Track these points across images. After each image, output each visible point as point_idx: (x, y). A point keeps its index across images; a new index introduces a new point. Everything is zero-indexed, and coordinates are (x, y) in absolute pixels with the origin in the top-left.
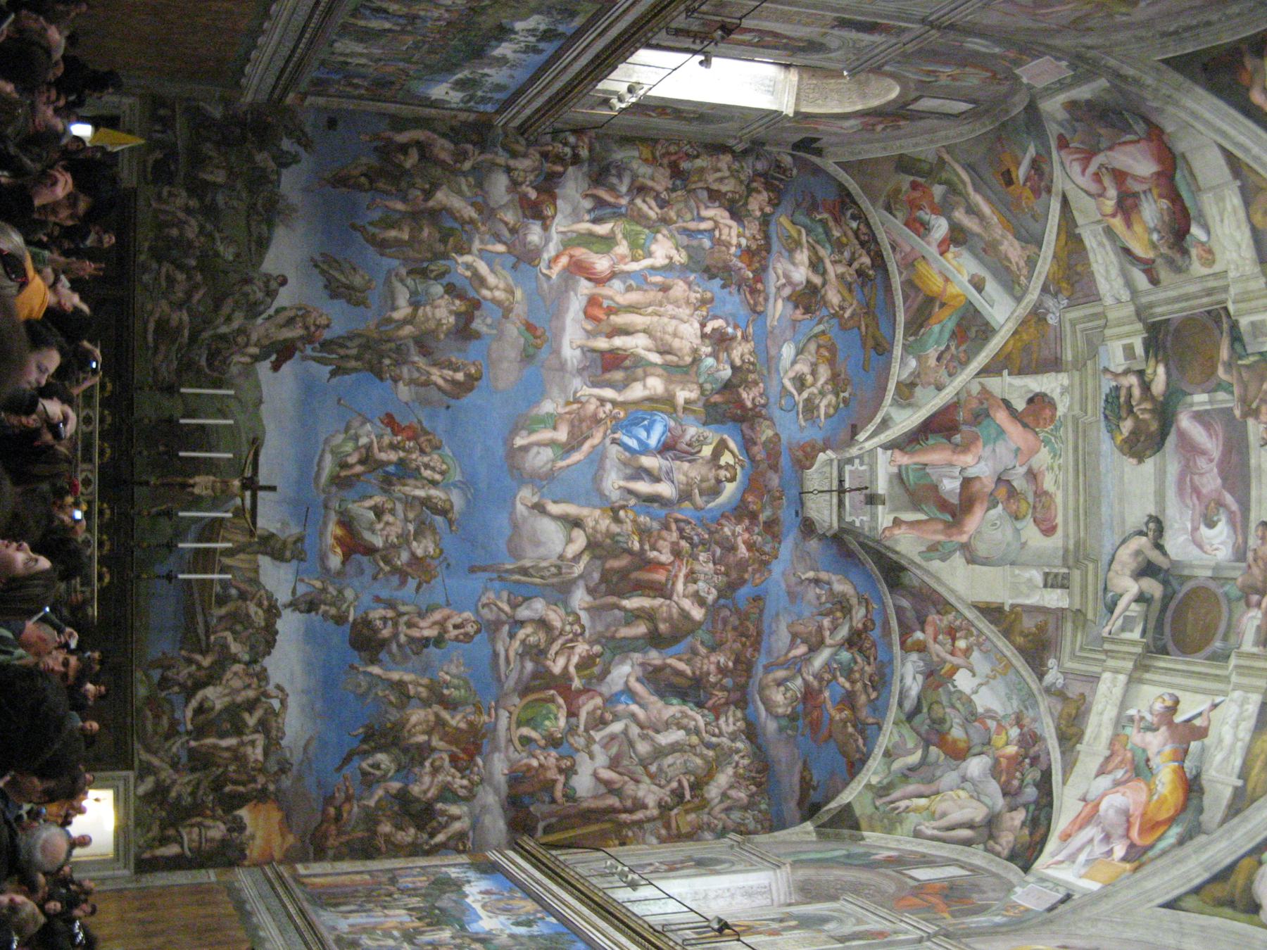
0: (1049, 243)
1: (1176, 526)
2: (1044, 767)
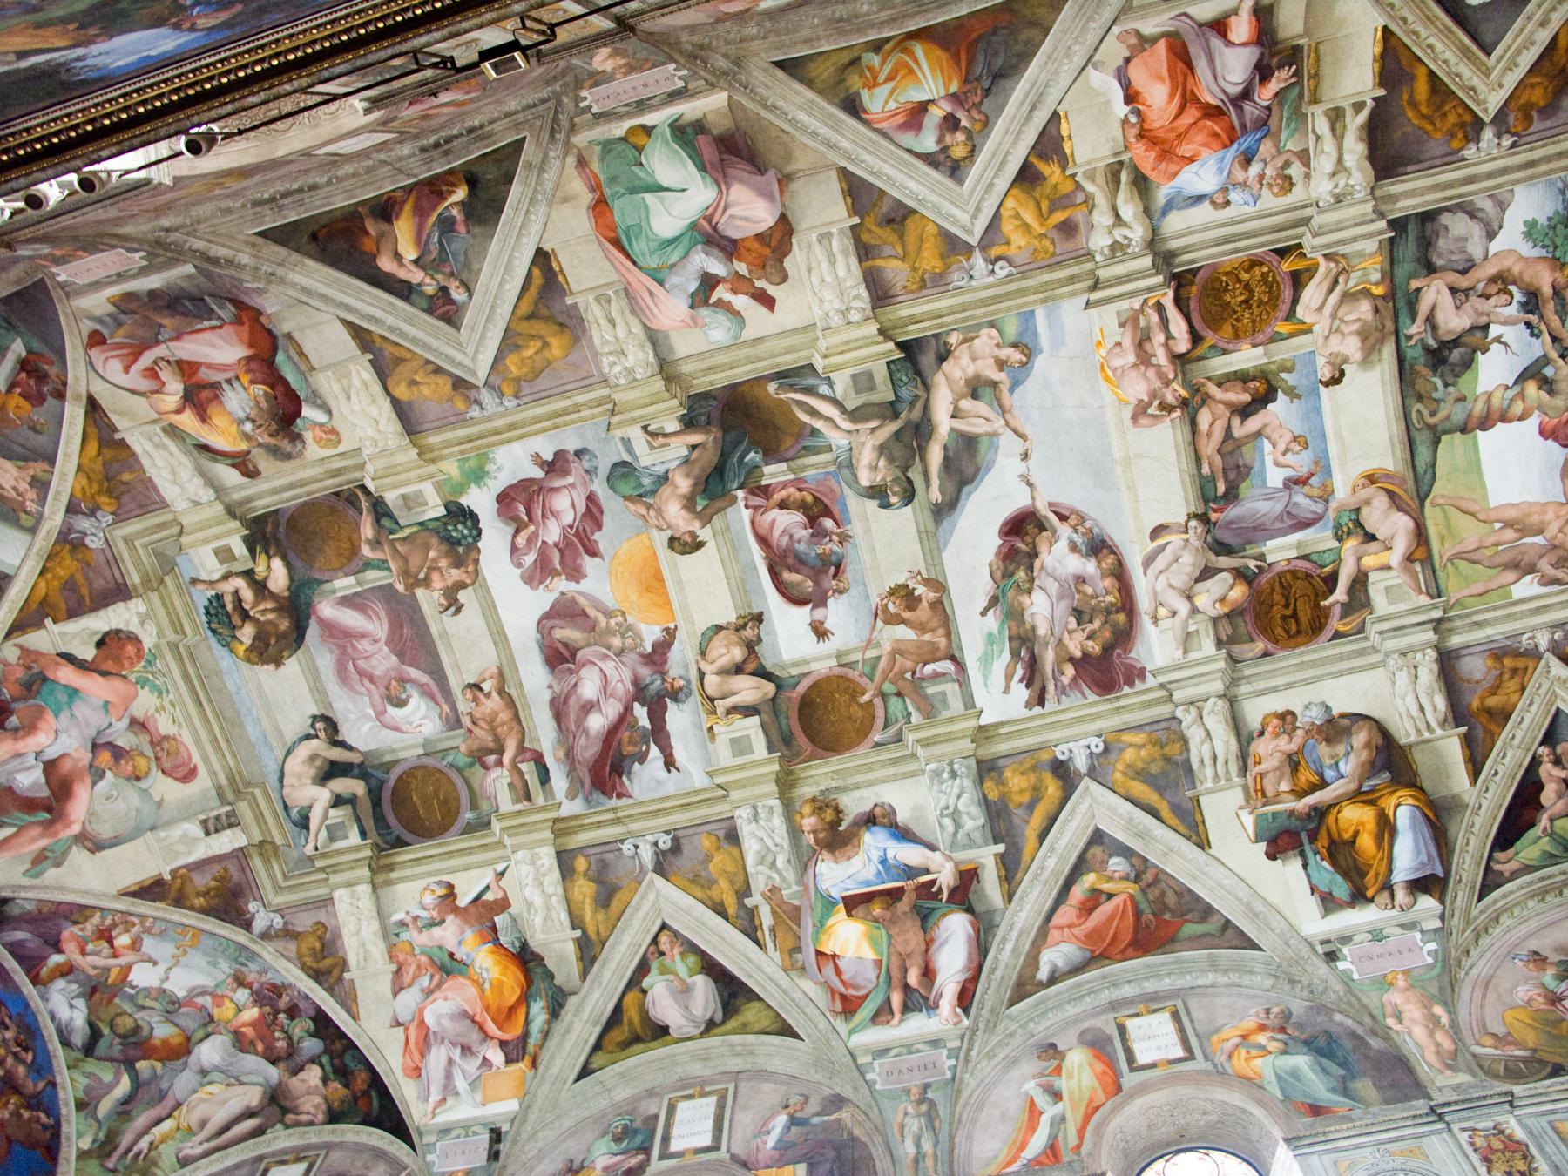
0: (67, 455)
1: (352, 716)
2: (312, 1013)
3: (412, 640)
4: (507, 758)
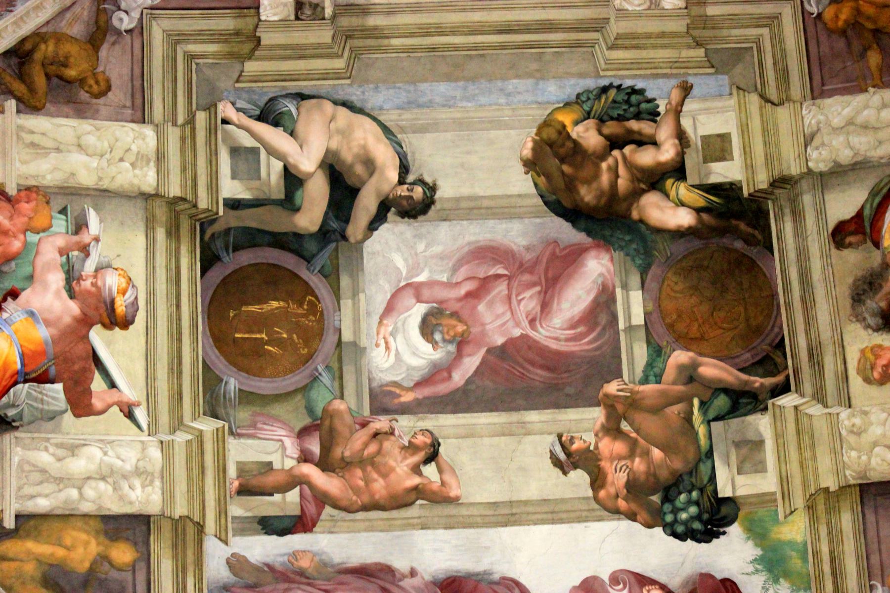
1: (421, 247)
3: (523, 376)
4: (310, 471)
